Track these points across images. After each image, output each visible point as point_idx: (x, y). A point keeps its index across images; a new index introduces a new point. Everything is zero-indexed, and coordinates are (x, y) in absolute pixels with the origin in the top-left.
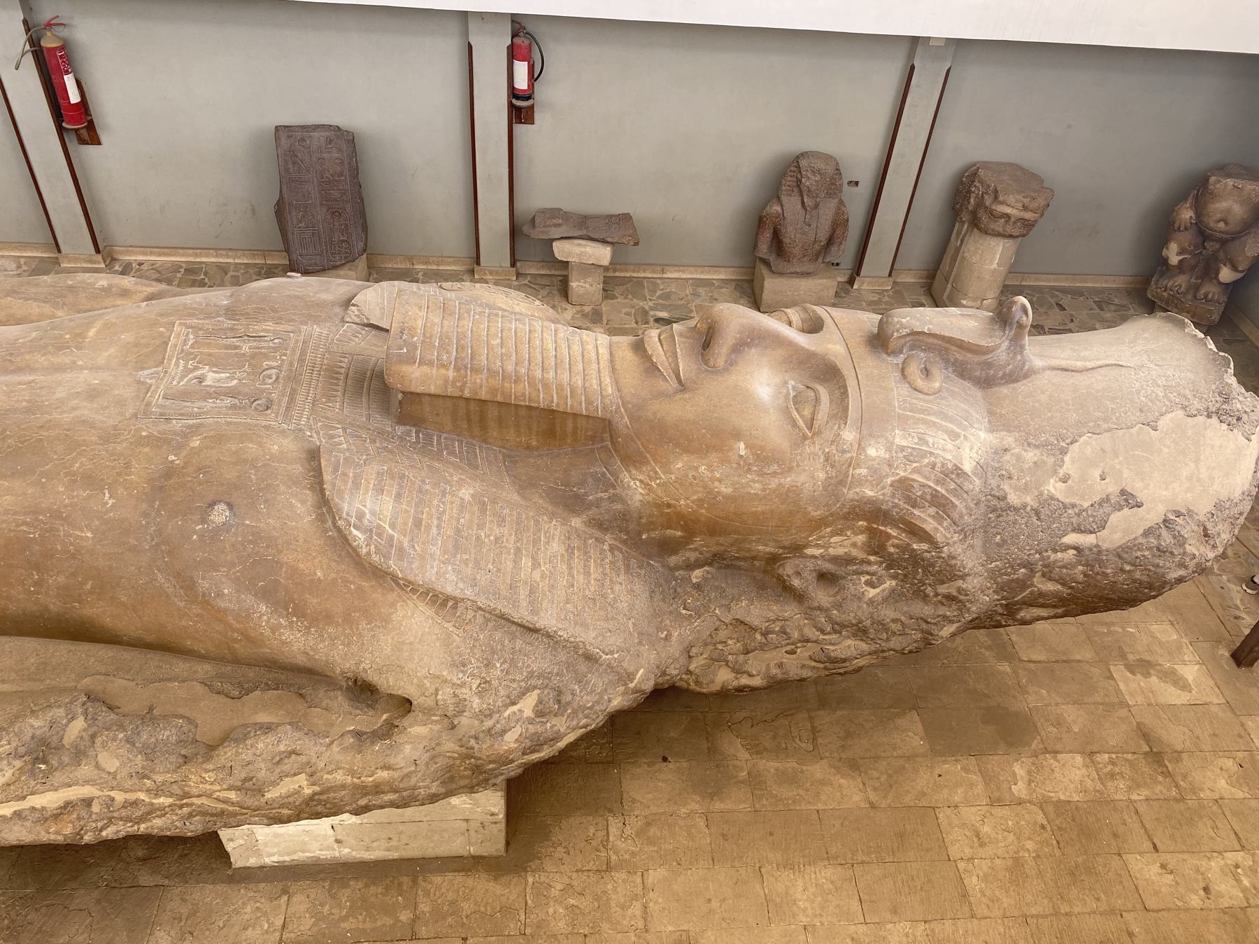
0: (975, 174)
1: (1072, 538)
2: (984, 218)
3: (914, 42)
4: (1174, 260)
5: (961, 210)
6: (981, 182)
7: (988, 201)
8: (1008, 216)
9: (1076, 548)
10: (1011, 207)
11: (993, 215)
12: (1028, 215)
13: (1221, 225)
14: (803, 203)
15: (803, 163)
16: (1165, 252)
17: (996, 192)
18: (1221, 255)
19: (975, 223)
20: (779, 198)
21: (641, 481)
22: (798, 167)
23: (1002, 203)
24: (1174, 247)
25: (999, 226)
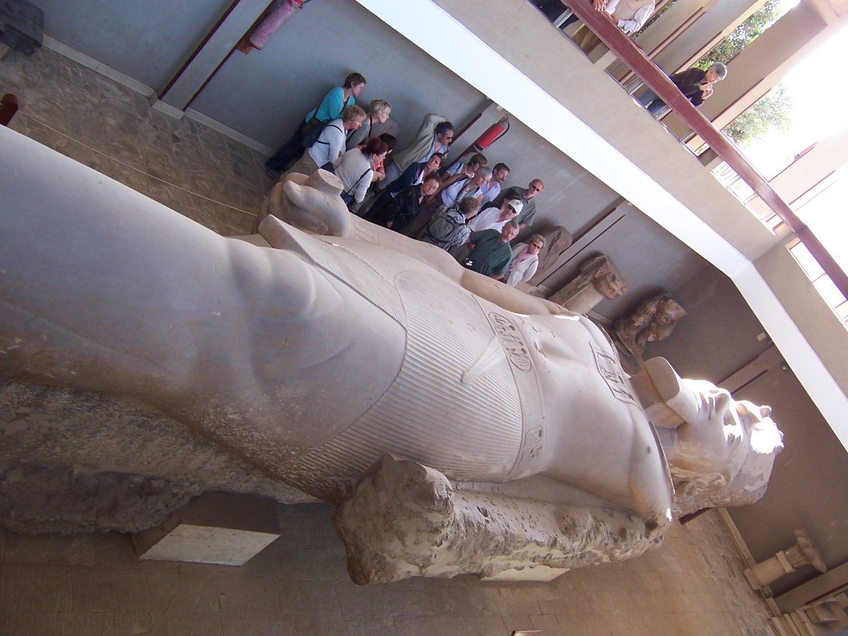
0: (603, 261)
1: (747, 487)
2: (603, 288)
3: (621, 200)
4: (636, 325)
5: (587, 273)
7: (609, 279)
10: (617, 287)
11: (609, 287)
12: (621, 294)
13: (664, 321)
14: (549, 250)
15: (562, 234)
16: (634, 318)
17: (614, 279)
24: (642, 319)
25: (608, 292)
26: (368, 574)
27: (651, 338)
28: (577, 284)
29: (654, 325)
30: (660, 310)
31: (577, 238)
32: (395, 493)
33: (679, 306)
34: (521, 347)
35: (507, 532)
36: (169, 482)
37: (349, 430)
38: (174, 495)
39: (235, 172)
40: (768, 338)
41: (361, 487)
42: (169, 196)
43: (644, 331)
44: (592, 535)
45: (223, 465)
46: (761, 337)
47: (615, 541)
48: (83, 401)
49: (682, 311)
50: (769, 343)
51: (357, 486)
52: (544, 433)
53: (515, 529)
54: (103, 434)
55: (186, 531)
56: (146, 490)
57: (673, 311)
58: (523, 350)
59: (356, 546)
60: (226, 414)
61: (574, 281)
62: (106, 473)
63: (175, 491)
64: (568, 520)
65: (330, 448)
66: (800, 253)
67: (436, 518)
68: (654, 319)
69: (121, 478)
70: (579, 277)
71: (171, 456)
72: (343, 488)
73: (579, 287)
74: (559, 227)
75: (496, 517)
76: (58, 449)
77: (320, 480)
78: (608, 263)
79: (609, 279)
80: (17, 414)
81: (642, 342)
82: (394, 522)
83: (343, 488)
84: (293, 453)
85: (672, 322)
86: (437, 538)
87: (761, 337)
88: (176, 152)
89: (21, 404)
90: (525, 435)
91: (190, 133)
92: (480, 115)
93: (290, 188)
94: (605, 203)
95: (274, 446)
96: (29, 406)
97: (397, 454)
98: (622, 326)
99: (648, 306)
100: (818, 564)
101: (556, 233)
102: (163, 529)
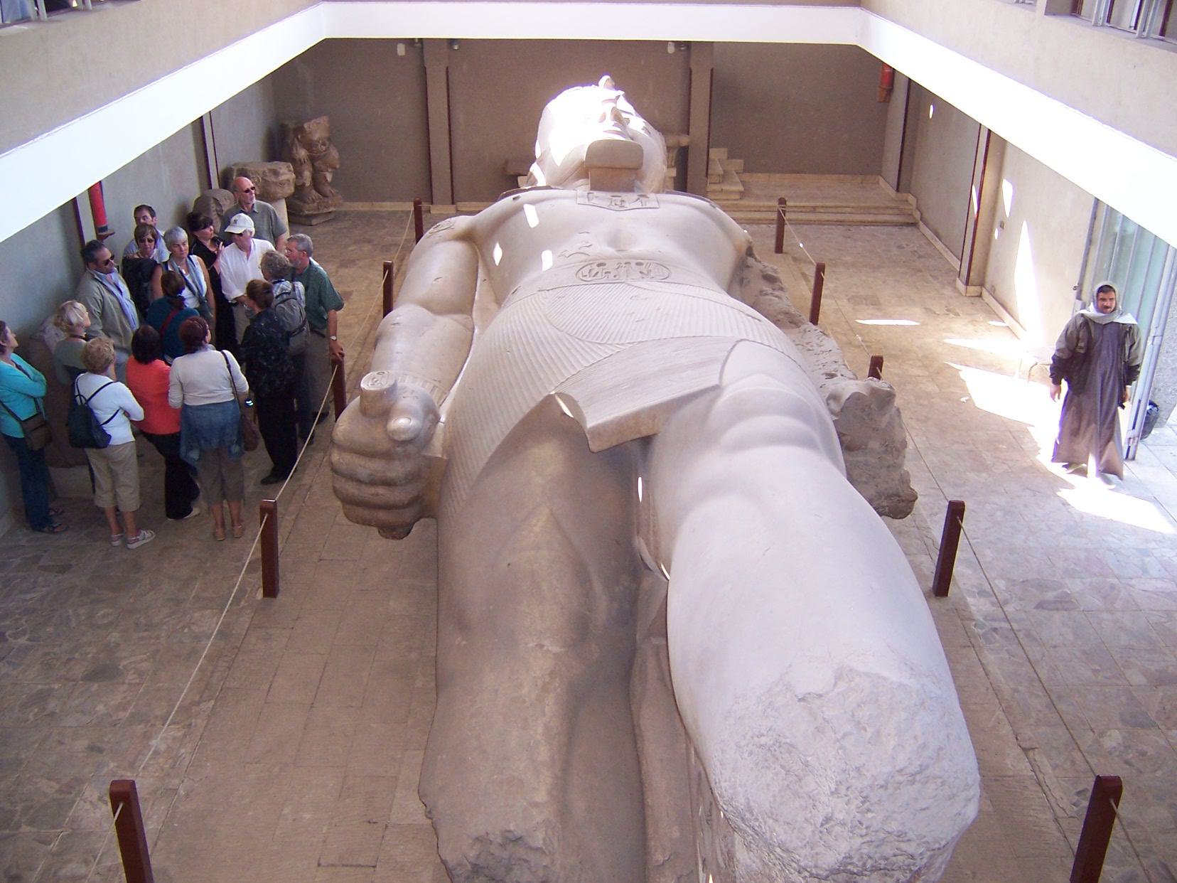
2: (279, 191)
4: (308, 184)
7: (273, 179)
11: (282, 184)
18: (323, 167)
27: (329, 177)
29: (317, 164)
30: (309, 146)
33: (317, 120)
34: (633, 265)
40: (410, 42)
42: (142, 661)
43: (316, 184)
46: (401, 50)
49: (324, 120)
50: (417, 46)
57: (317, 129)
58: (638, 264)
59: (889, 497)
68: (312, 159)
79: (273, 179)
81: (327, 189)
85: (329, 139)
88: (29, 640)
93: (405, 431)
98: (298, 202)
99: (297, 157)
100: (684, 140)
101: (213, 206)
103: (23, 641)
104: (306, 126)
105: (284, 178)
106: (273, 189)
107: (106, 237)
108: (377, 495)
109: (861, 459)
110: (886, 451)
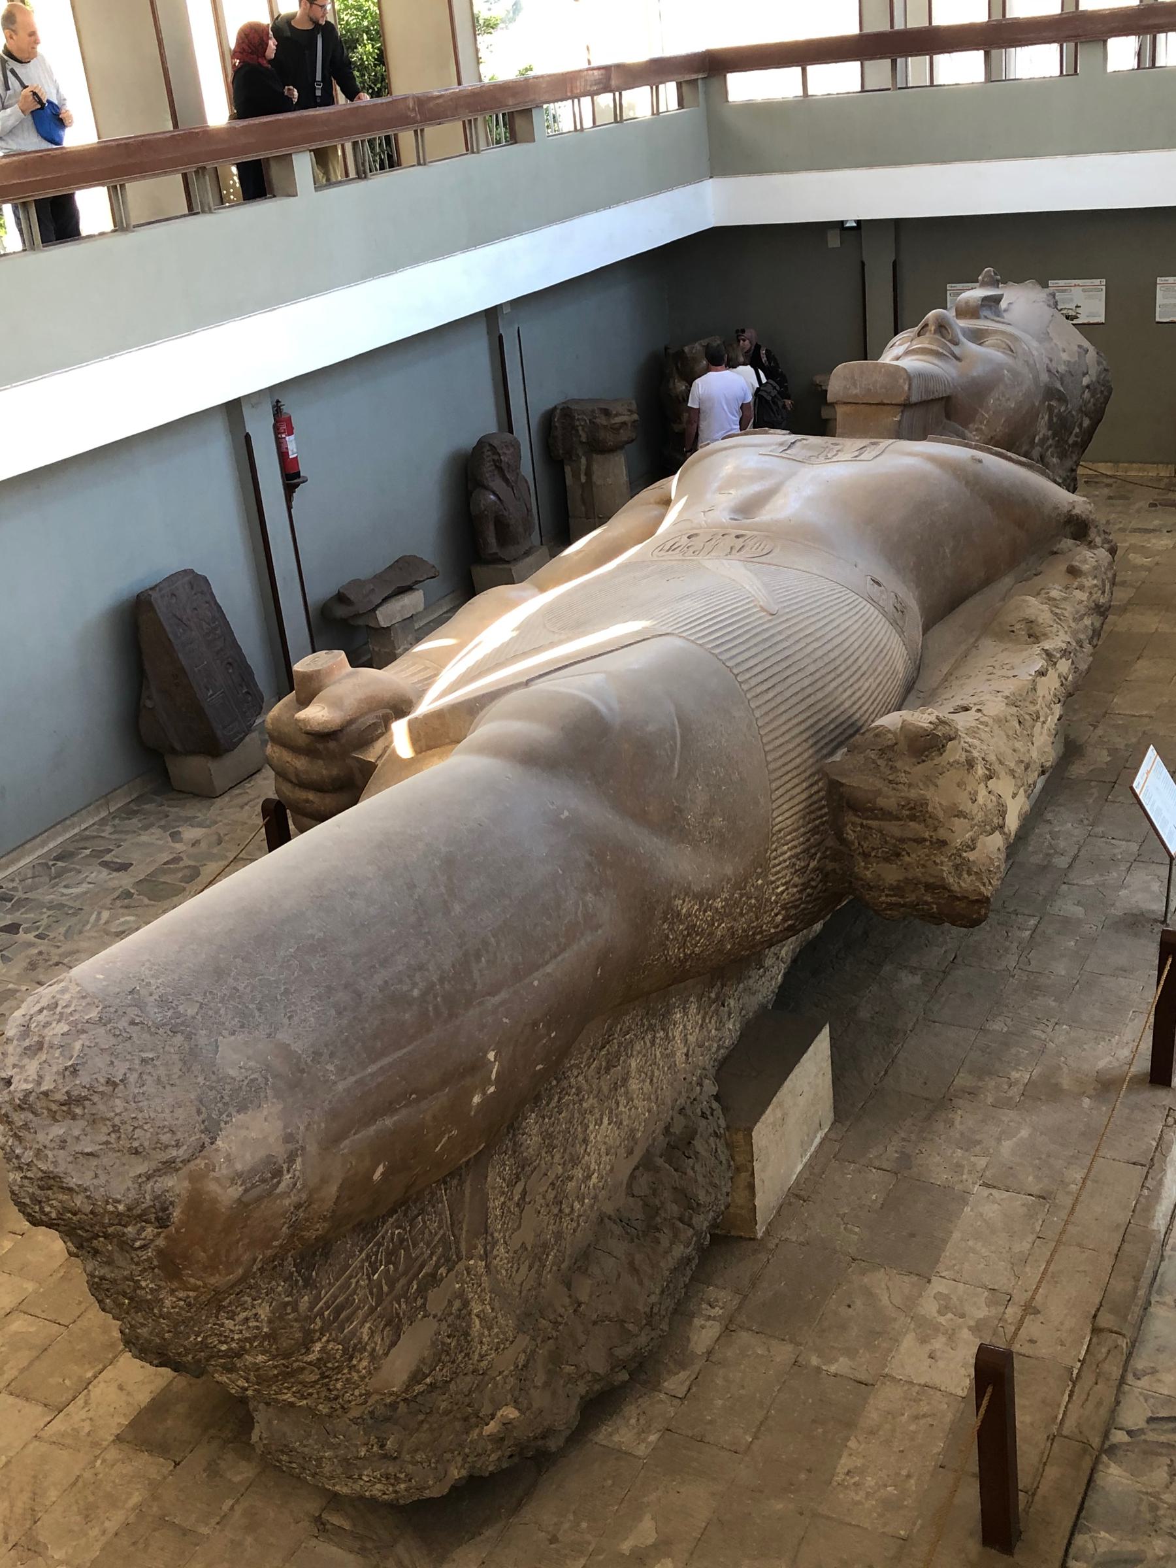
1: (1086, 381)
2: (610, 439)
3: (491, 315)
6: (583, 413)
7: (602, 420)
8: (624, 423)
9: (1088, 387)
11: (616, 429)
12: (635, 417)
14: (506, 481)
15: (495, 443)
19: (598, 447)
20: (486, 488)
21: (977, 430)
22: (493, 448)
23: (616, 415)
26: (981, 894)
28: (576, 475)
31: (507, 423)
32: (890, 782)
35: (1007, 697)
36: (682, 1111)
37: (774, 786)
38: (703, 1115)
39: (118, 870)
41: (850, 835)
44: (1057, 611)
45: (699, 1018)
46: (834, 241)
47: (1081, 588)
48: (548, 1104)
51: (842, 840)
52: (879, 579)
53: (1009, 687)
54: (591, 1127)
55: (762, 1134)
56: (677, 1146)
59: (929, 887)
60: (679, 914)
61: (569, 481)
62: (632, 1177)
63: (699, 1111)
64: (1018, 626)
65: (780, 831)
66: (744, 87)
67: (954, 753)
69: (646, 1163)
70: (568, 469)
71: (656, 1073)
72: (830, 866)
73: (583, 479)
74: (481, 443)
75: (975, 699)
76: (577, 1206)
77: (806, 885)
78: (574, 407)
80: (518, 1205)
82: (929, 809)
83: (830, 866)
84: (760, 882)
86: (980, 771)
87: (834, 241)
89: (512, 1184)
90: (871, 600)
91: (9, 905)
92: (248, 437)
94: (478, 349)
95: (742, 896)
96: (518, 1179)
97: (832, 753)
102: (741, 1167)
103: (30, 937)
104: (686, 349)
105: (618, 420)
106: (602, 435)
107: (297, 485)
108: (307, 801)
109: (874, 823)
110: (913, 818)
